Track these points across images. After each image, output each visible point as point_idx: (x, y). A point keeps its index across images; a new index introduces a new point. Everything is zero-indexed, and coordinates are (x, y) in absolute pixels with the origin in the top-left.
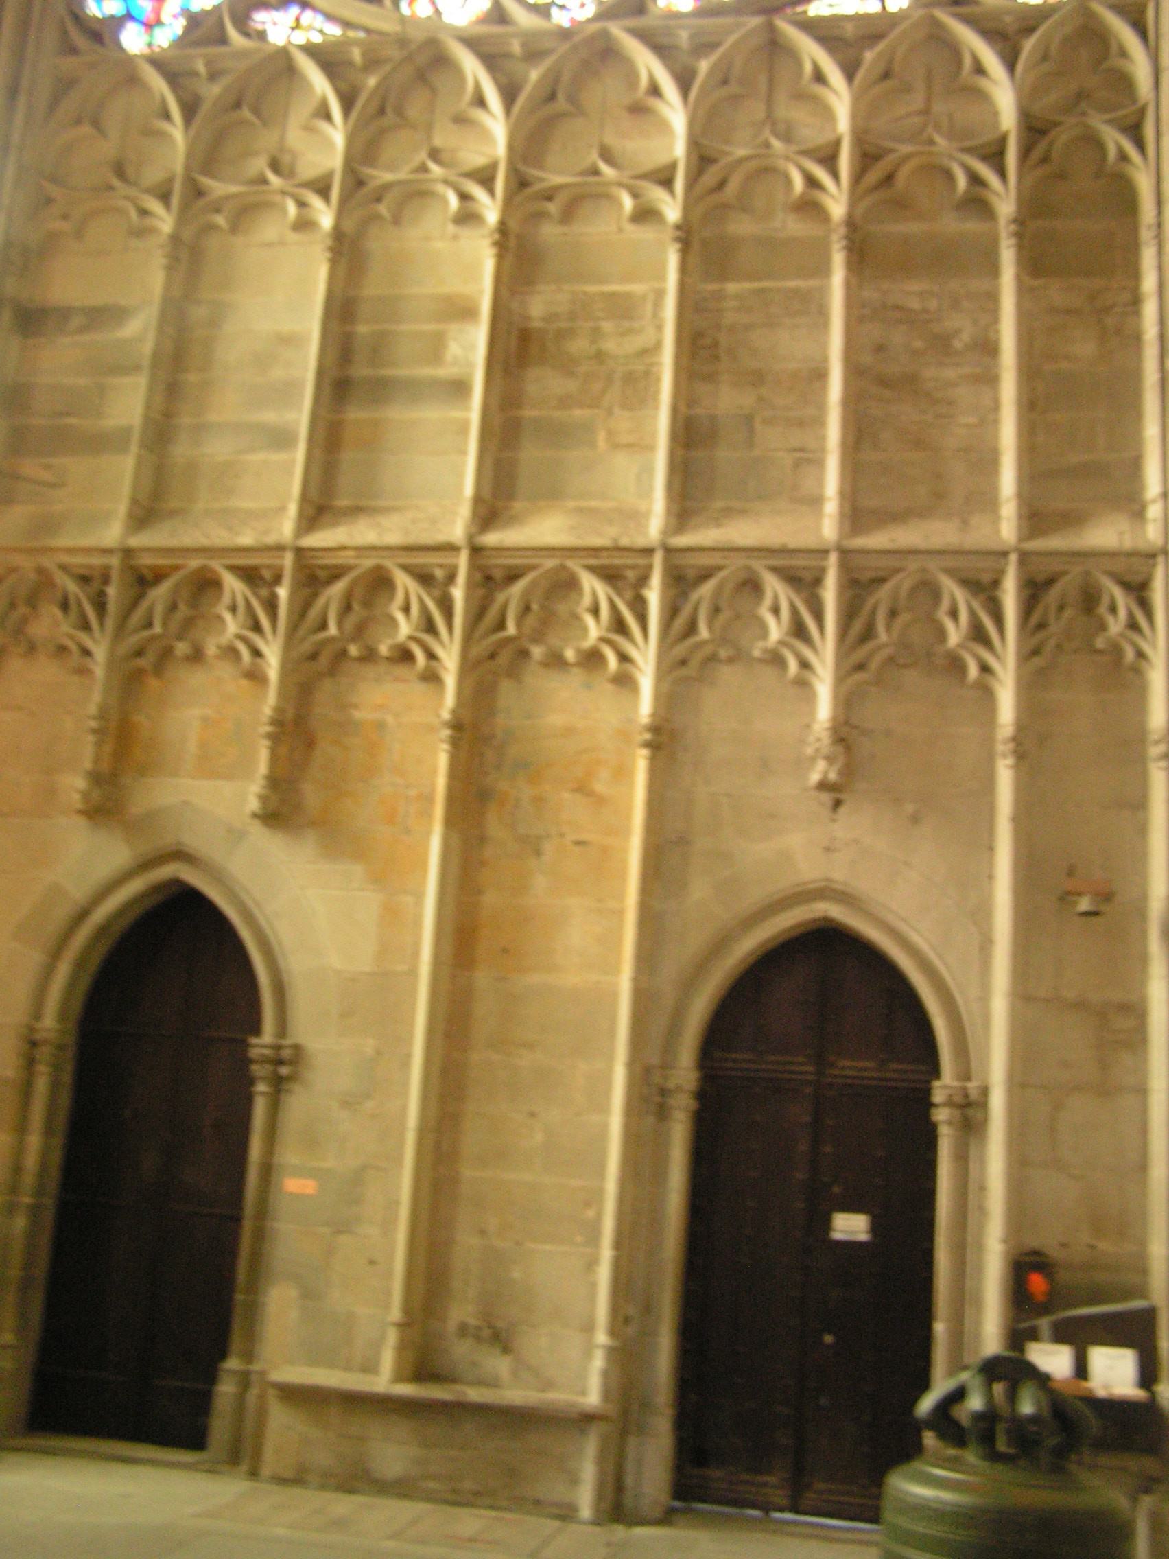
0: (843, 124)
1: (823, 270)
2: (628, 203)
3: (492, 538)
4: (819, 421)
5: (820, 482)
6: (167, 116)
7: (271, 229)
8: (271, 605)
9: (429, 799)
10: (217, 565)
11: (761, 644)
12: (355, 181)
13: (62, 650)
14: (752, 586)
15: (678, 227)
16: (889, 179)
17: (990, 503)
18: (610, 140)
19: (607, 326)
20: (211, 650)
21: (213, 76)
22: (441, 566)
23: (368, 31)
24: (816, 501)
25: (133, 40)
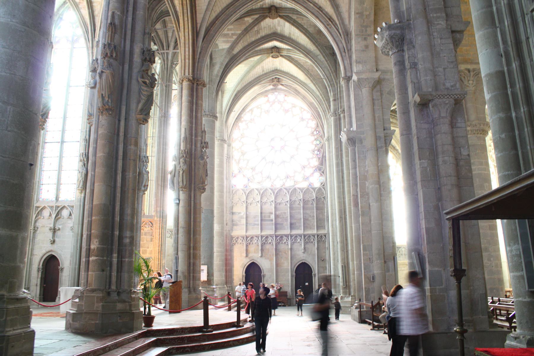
1: (301, 210)
3: (276, 234)
4: (301, 223)
9: (273, 254)
24: (301, 229)
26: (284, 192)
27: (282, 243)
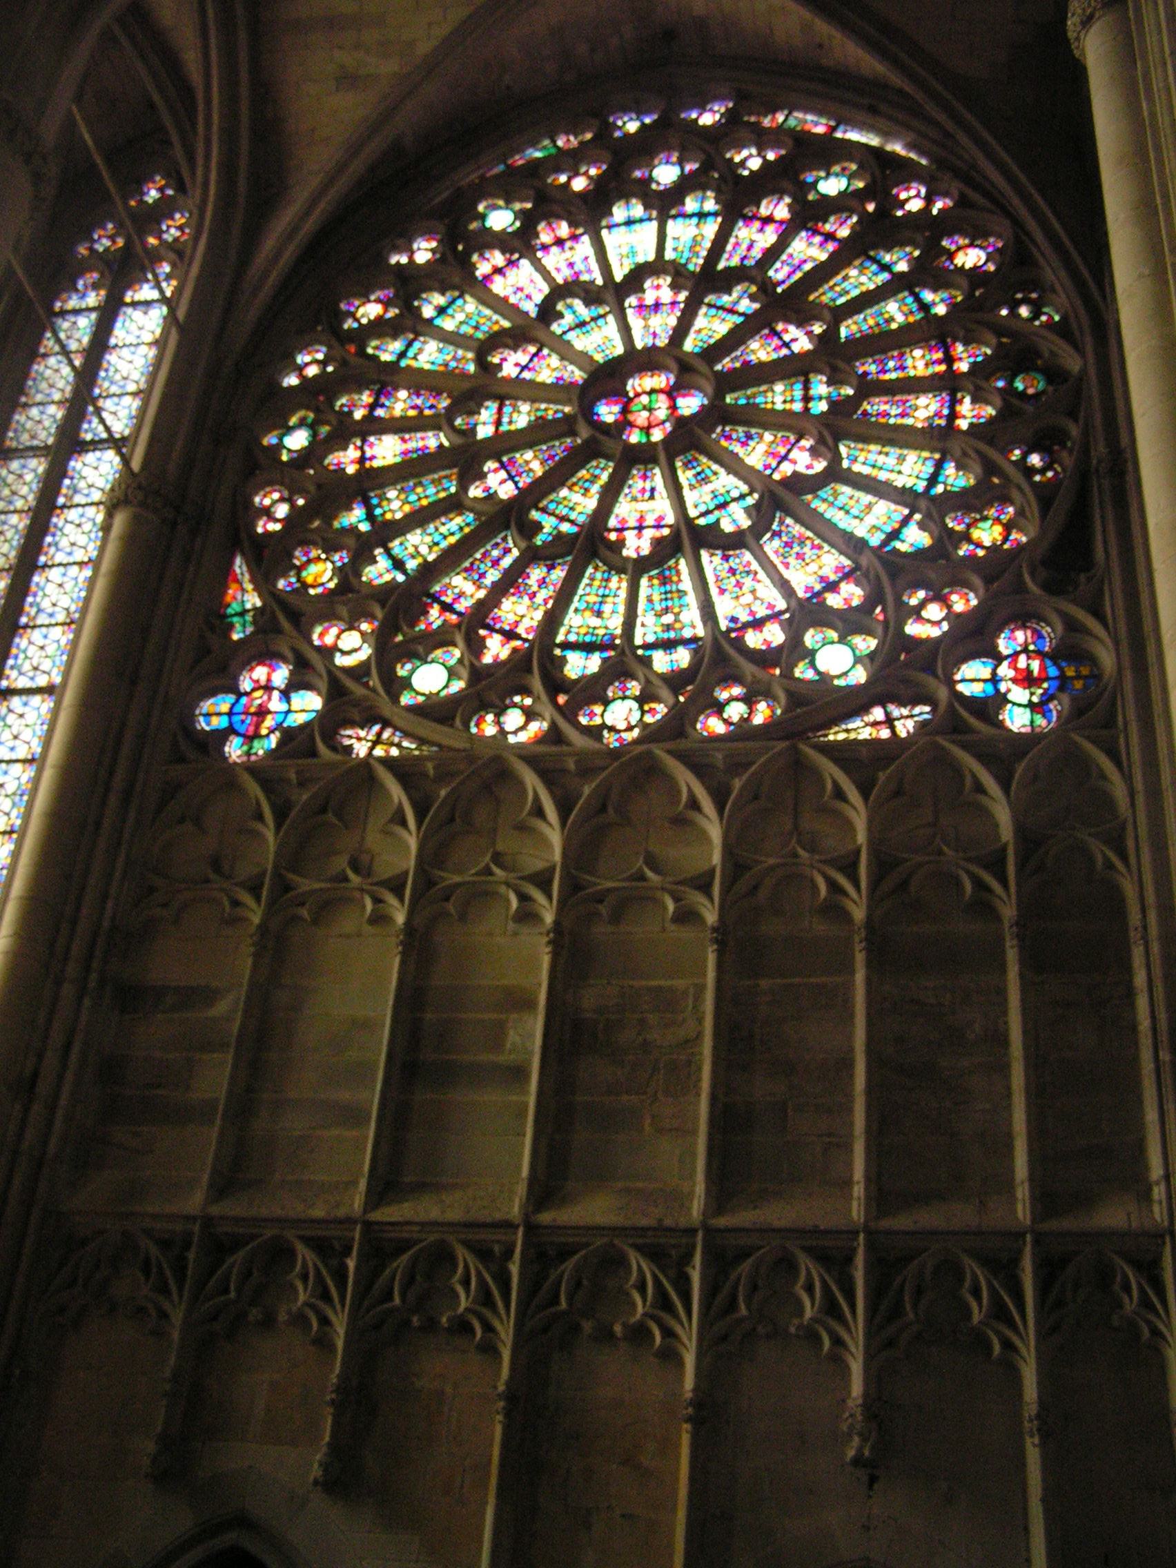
0: (861, 837)
2: (671, 906)
3: (546, 1218)
5: (849, 1165)
6: (260, 817)
7: (349, 922)
8: (340, 1276)
10: (290, 1234)
11: (796, 1321)
12: (426, 881)
13: (141, 1310)
14: (787, 1265)
15: (715, 930)
16: (903, 885)
17: (1008, 1185)
18: (655, 848)
19: (652, 1018)
20: (282, 1317)
21: (302, 784)
22: (498, 1242)
23: (439, 745)
25: (234, 749)
26: (674, 790)
27: (605, 1335)
